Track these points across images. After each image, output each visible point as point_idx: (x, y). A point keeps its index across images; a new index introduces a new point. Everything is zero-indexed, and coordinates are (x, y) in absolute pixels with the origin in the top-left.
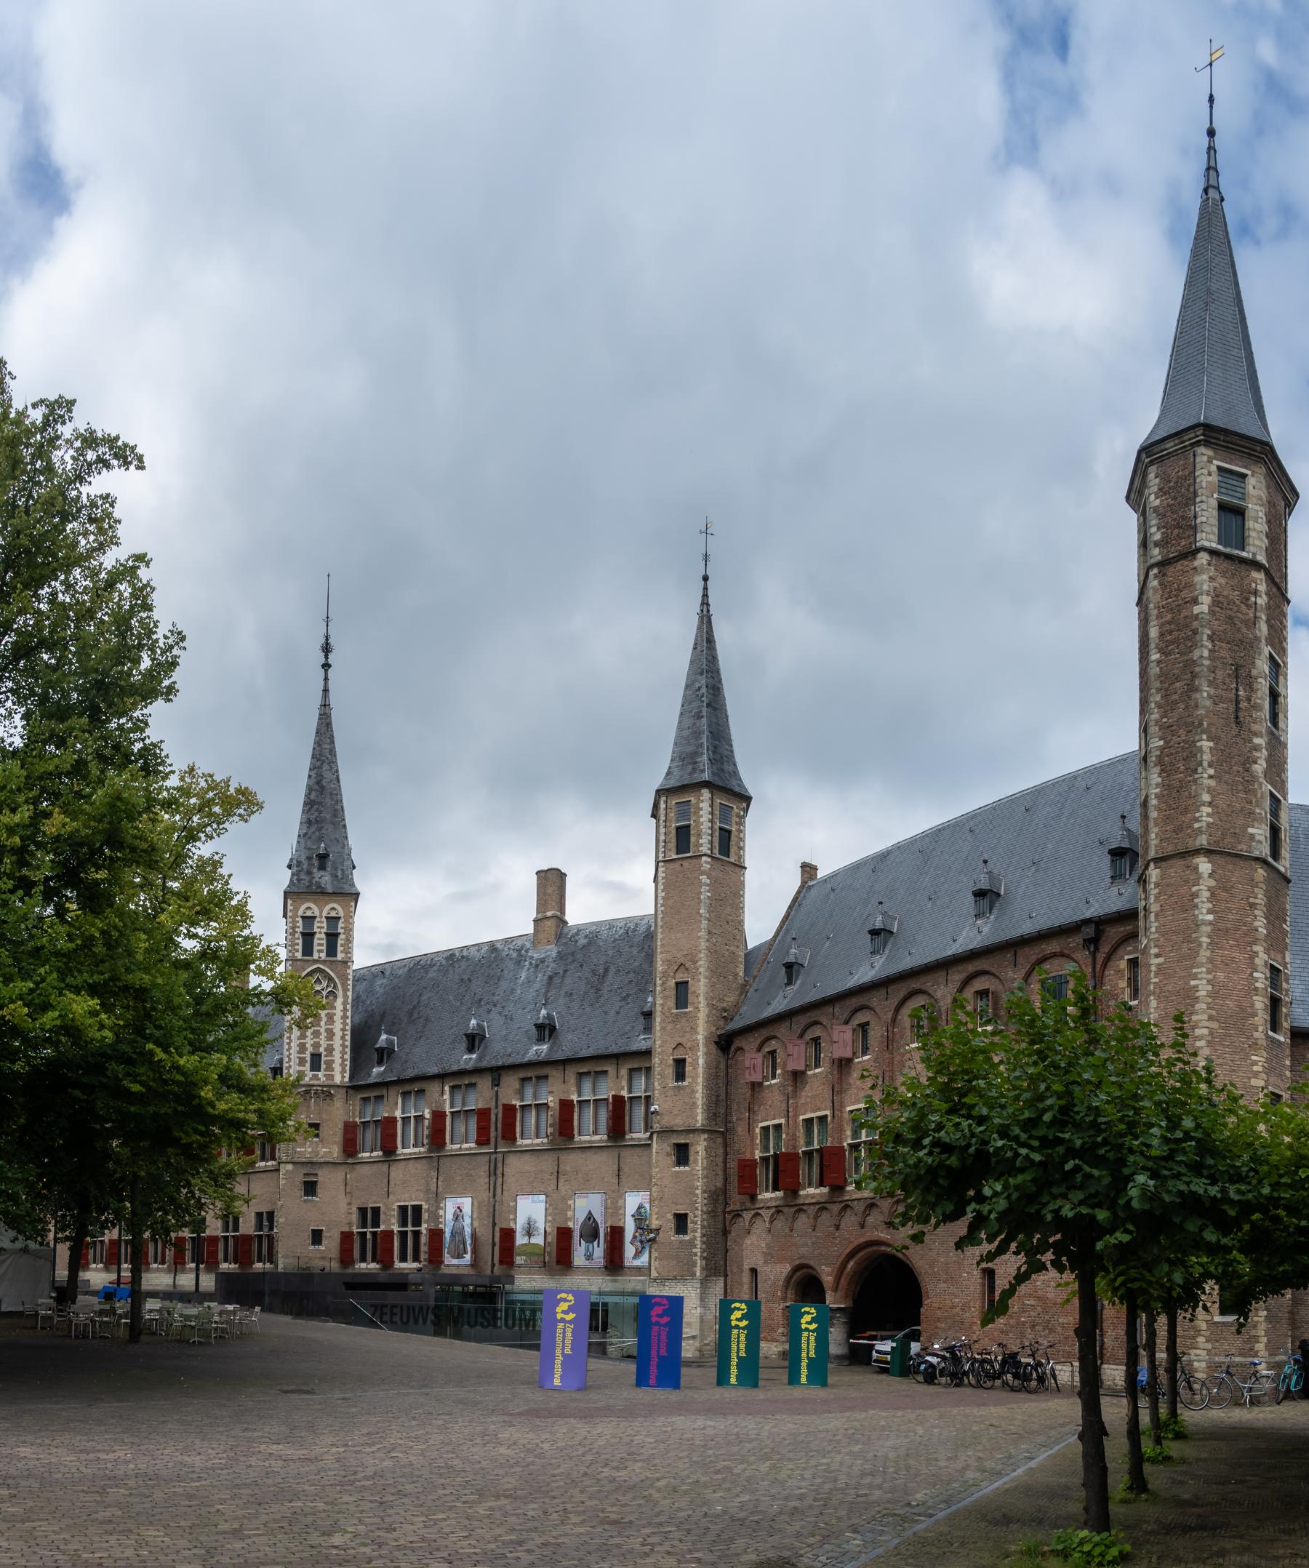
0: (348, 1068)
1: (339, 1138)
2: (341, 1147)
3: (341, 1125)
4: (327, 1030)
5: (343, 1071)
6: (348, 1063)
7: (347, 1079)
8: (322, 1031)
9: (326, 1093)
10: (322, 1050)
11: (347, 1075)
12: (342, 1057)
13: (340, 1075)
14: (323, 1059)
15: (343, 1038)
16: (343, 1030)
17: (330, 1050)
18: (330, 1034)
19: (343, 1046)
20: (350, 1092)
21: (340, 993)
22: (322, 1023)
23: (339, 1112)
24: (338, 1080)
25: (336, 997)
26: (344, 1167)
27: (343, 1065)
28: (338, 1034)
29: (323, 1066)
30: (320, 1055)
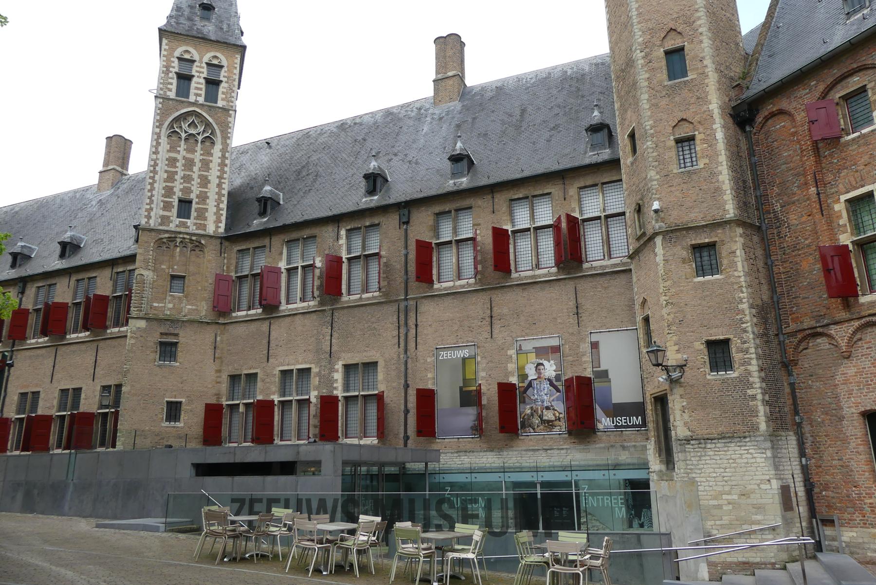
0: (223, 218)
1: (208, 294)
2: (211, 304)
3: (211, 280)
4: (200, 176)
5: (218, 221)
6: (224, 213)
7: (222, 230)
8: (195, 176)
9: (196, 244)
10: (193, 196)
11: (222, 225)
12: (217, 206)
13: (214, 222)
14: (194, 206)
15: (219, 185)
16: (220, 178)
17: (203, 197)
18: (205, 182)
19: (219, 194)
20: (226, 244)
21: (218, 140)
22: (195, 169)
23: (209, 265)
24: (211, 229)
25: (213, 143)
26: (214, 327)
27: (218, 214)
28: (214, 181)
29: (194, 214)
30: (190, 202)
